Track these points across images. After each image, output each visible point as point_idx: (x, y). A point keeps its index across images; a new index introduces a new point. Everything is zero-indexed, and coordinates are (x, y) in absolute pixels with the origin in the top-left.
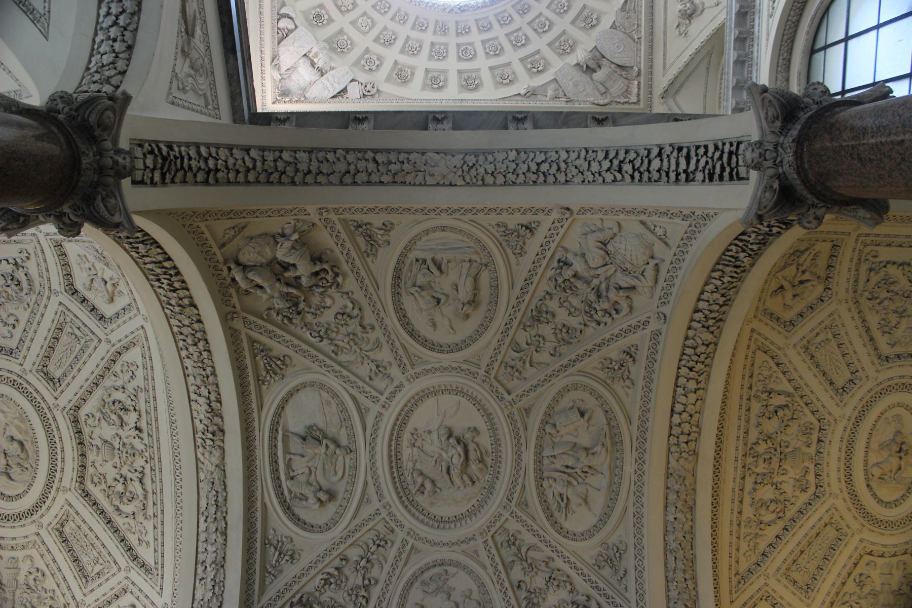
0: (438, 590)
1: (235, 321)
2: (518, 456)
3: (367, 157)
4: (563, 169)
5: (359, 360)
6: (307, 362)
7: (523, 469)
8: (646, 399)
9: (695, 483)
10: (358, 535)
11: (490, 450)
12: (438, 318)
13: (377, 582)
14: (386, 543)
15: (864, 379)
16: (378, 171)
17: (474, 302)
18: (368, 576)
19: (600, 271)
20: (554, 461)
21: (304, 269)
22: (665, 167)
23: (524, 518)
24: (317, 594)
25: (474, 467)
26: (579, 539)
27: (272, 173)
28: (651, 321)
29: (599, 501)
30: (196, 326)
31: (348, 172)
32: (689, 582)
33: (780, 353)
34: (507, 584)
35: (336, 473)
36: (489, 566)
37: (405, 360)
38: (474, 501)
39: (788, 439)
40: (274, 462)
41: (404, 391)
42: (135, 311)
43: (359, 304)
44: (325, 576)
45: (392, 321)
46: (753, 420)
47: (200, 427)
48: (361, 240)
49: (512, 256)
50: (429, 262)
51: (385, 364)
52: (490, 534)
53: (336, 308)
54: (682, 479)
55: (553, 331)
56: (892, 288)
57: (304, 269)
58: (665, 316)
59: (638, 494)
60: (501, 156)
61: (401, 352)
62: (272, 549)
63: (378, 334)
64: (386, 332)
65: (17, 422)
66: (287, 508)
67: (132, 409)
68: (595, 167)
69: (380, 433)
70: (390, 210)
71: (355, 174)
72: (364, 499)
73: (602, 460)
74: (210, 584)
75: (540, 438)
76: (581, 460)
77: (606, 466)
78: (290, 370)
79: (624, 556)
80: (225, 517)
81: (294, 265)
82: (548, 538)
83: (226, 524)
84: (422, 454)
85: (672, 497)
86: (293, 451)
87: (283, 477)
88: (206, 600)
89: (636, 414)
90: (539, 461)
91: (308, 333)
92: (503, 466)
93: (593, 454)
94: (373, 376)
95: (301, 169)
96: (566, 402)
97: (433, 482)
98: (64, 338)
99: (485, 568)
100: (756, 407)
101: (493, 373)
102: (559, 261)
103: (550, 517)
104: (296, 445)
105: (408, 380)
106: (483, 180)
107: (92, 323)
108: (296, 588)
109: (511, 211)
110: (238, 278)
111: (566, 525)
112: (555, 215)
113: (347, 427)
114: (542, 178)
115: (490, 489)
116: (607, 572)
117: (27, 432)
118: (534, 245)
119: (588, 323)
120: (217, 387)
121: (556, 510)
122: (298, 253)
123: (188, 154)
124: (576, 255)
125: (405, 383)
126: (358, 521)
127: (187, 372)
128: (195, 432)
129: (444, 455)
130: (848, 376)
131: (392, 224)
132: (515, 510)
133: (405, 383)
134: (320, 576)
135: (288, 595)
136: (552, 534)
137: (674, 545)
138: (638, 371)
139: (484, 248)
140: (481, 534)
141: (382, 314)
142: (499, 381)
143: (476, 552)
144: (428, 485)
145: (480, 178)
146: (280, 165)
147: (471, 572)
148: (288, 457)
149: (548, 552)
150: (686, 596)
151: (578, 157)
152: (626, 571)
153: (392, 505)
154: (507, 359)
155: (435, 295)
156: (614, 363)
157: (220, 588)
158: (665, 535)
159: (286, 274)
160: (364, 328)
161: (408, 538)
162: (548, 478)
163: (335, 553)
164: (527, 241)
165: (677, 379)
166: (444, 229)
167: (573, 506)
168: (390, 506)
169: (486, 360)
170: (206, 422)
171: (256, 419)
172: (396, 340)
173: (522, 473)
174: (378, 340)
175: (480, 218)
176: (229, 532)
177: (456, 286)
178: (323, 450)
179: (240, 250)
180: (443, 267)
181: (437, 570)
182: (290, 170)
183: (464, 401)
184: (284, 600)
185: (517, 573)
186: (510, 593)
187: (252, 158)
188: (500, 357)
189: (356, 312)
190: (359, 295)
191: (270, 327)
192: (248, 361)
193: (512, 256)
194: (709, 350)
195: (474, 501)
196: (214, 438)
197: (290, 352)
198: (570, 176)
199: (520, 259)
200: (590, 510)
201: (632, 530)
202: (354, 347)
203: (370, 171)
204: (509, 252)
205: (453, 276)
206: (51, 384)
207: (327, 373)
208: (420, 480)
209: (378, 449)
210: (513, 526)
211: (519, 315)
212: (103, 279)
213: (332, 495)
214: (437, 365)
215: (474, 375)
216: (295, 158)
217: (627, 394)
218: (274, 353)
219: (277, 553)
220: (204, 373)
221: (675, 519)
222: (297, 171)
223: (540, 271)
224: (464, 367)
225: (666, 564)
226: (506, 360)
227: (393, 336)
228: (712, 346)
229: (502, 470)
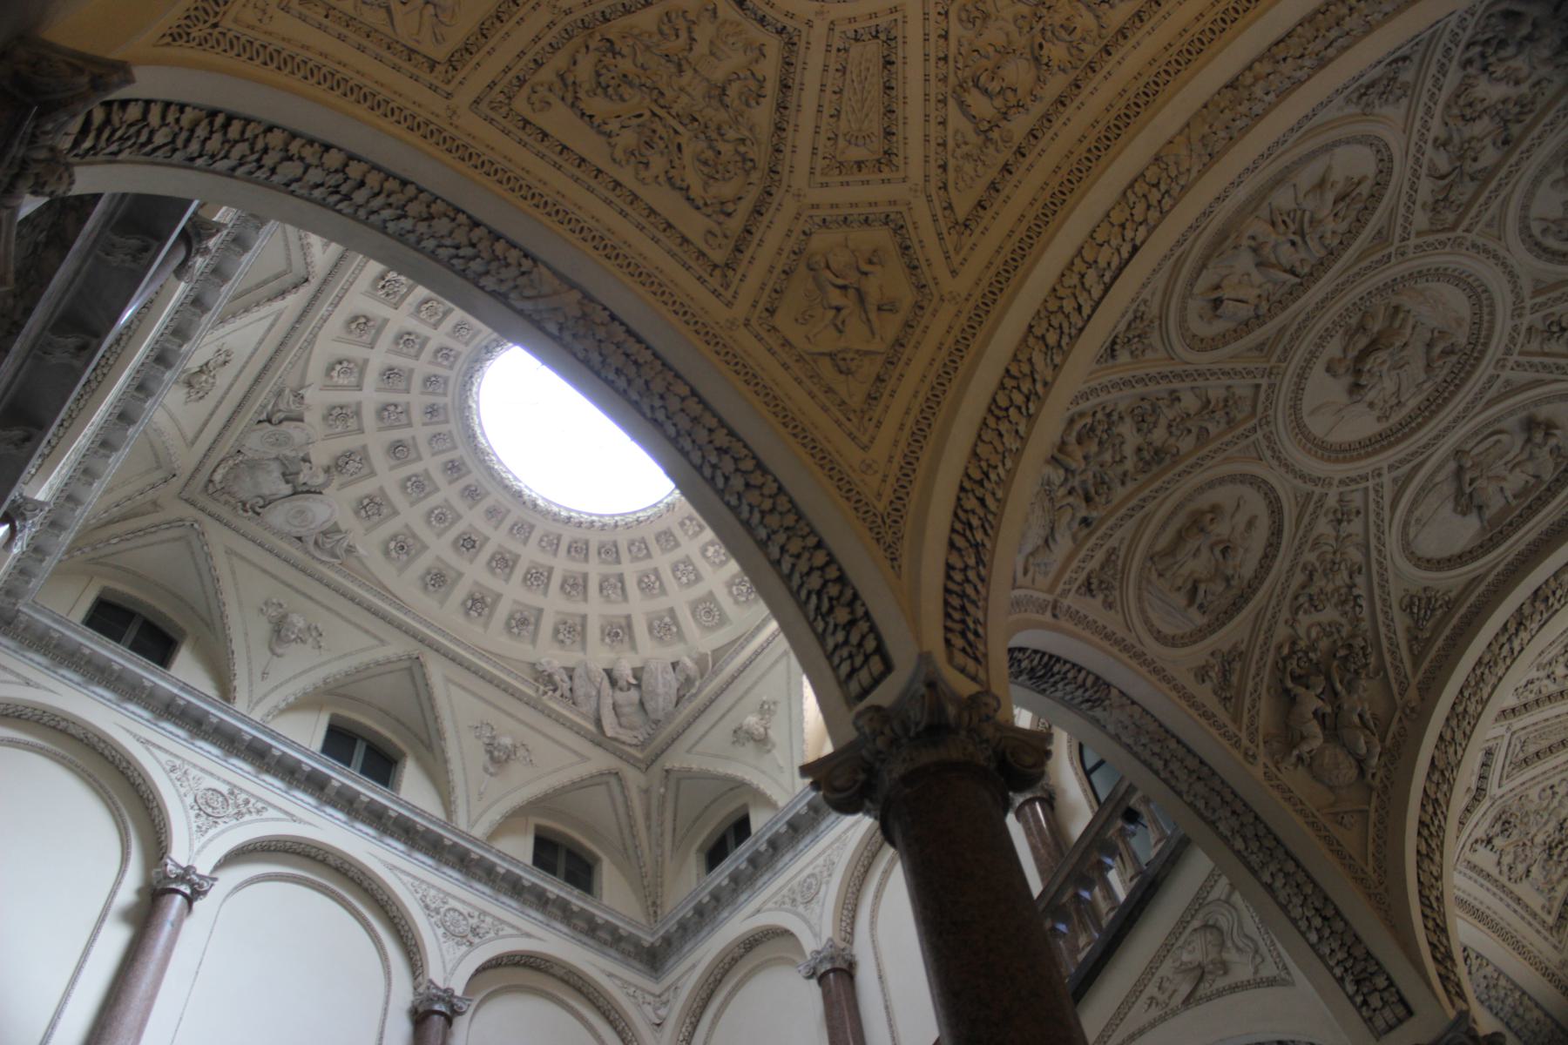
11: (1341, 331)
15: (838, 29)
23: (1400, 221)
30: (1448, 737)
33: (933, 190)
36: (1500, 198)
39: (1012, 28)
41: (1343, 476)
45: (1281, 563)
46: (1037, 109)
48: (1235, 679)
49: (1122, 553)
51: (1331, 516)
52: (1452, 235)
56: (710, 154)
57: (1311, 702)
63: (1310, 557)
64: (1299, 551)
72: (1512, 390)
90: (1313, 277)
97: (1430, 346)
98: (1532, 749)
100: (1019, 125)
115: (1391, 286)
121: (1358, 201)
125: (1336, 482)
130: (855, 50)
136: (1401, 171)
141: (1283, 579)
148: (1514, 503)
159: (1328, 709)
167: (1339, 187)
169: (1243, 443)
171: (1495, 572)
174: (1312, 549)
180: (1189, 585)
183: (1307, 405)
190: (1285, 614)
191: (1388, 657)
192: (1440, 643)
193: (1122, 553)
197: (1396, 612)
204: (1120, 563)
210: (1421, 219)
213: (1530, 424)
224: (1268, 453)
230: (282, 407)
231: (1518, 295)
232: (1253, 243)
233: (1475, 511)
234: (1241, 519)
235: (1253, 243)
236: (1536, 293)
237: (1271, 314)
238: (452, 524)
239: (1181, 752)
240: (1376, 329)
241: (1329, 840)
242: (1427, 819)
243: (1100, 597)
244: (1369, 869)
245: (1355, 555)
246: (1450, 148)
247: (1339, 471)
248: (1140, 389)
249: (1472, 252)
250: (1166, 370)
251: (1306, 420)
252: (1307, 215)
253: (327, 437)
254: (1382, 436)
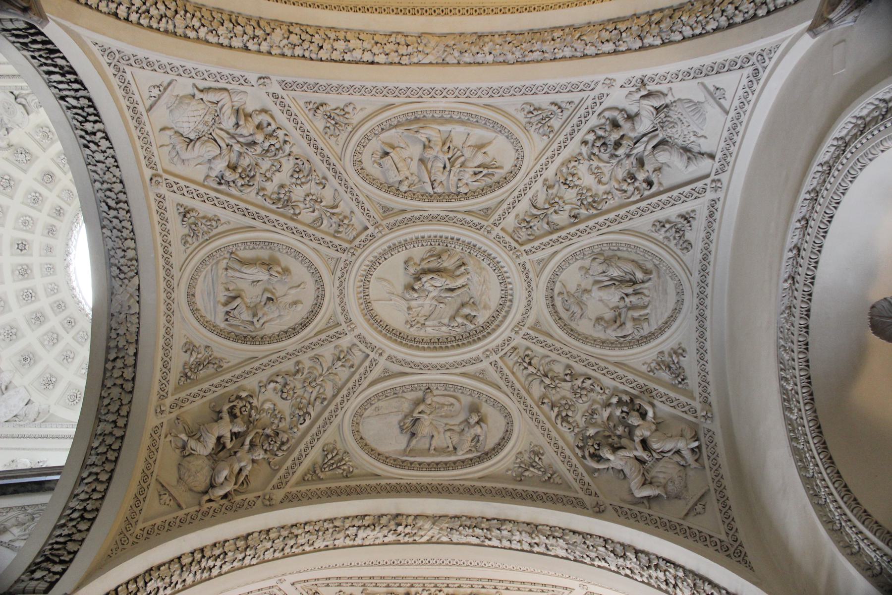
0: (580, 303)
1: (274, 497)
2: (432, 219)
3: (110, 368)
4: (109, 186)
5: (331, 377)
6: (331, 429)
7: (447, 213)
8: (362, 90)
9: (454, 34)
10: (517, 385)
11: (429, 247)
12: (289, 299)
13: (568, 367)
14: (527, 356)
16: (123, 357)
17: (268, 264)
18: (562, 376)
19: (223, 145)
20: (438, 181)
21: (225, 428)
22: (72, 93)
23: (500, 211)
24: (576, 430)
25: (448, 263)
26: (521, 154)
27: (107, 458)
28: (271, 91)
29: (479, 134)
30: (272, 535)
31: (122, 385)
32: (556, 35)
34: (573, 230)
35: (452, 404)
37: (332, 332)
38: (484, 264)
40: (437, 466)
41: (364, 333)
43: (272, 376)
44: (559, 421)
45: (290, 344)
47: (391, 537)
49: (220, 229)
50: (228, 308)
53: (277, 399)
54: (448, 49)
55: (299, 187)
57: (225, 428)
58: (260, 78)
59: (468, 94)
60: (110, 244)
61: (323, 336)
62: (526, 474)
63: (305, 359)
64: (304, 350)
66: (486, 456)
68: (99, 156)
69: (409, 358)
70: (167, 346)
71: (124, 379)
72: (480, 377)
73: (433, 132)
74: (551, 541)
75: (414, 197)
76: (435, 154)
77: (442, 128)
78: (339, 446)
79: (537, 106)
80: (488, 520)
81: (219, 438)
82: (522, 187)
83: (494, 519)
84: (433, 317)
85: (467, 58)
86: (427, 446)
87: (453, 458)
88: (566, 547)
89: (381, 101)
90: (439, 197)
91: (300, 426)
92: (444, 234)
93: (429, 141)
94: (348, 364)
95: (110, 430)
96: (374, 171)
97: (463, 305)
99: (556, 253)
101: (345, 245)
102: (220, 184)
103: (499, 184)
104: (420, 443)
105: (353, 329)
106: (131, 260)
108: (568, 452)
109: (165, 233)
110: (222, 492)
111: (508, 167)
112: (163, 190)
113: (403, 392)
114: (121, 205)
116: (556, 123)
118: (206, 209)
119: (287, 152)
120: (348, 518)
121: (491, 178)
122: (204, 435)
123: (57, 537)
124: (210, 168)
125: (356, 332)
126: (502, 384)
127: (331, 547)
128: (398, 543)
129: (432, 295)
131: (186, 344)
132: (491, 221)
133: (356, 332)
134: (559, 426)
135: (575, 461)
136: (518, 181)
137: (518, 54)
138: (334, 101)
139: (211, 256)
140: (518, 257)
141: (282, 354)
142: (355, 238)
143: (539, 262)
144: (466, 311)
145: (129, 263)
146: (102, 449)
147: (561, 268)
148: (432, 452)
149: (538, 186)
150: (569, 38)
151: (95, 172)
152: (552, 103)
153: (486, 348)
154: (332, 231)
155: (263, 303)
156: (328, 125)
157: (556, 531)
158: (508, 63)
160: (298, 371)
161: (522, 333)
162: (458, 188)
163: (536, 409)
164: (200, 215)
165: (335, 61)
166: (191, 296)
167: (487, 160)
168: (487, 350)
169: (332, 252)
170: (385, 532)
172: (310, 341)
173: (451, 215)
174: (311, 359)
175: (176, 261)
176: (502, 517)
177: (253, 282)
178: (425, 416)
179: (191, 490)
181: (558, 302)
182: (109, 440)
184: (578, 465)
185: (561, 218)
186: (582, 227)
187: (88, 476)
188: (328, 239)
189: (279, 379)
190: (263, 376)
194: (297, 30)
195: (484, 264)
196: (404, 524)
197: (319, 446)
198: (114, 179)
199: (223, 221)
200: (490, 143)
201: (507, 99)
202: (318, 381)
203: (122, 365)
204: (215, 231)
205: (244, 285)
207: (344, 410)
208: (459, 320)
209: (426, 361)
210: (510, 221)
211: (282, 220)
213: (474, 409)
214: (338, 300)
215: (347, 264)
216: (100, 435)
217: (361, 109)
218: (320, 461)
219: (532, 469)
220: (331, 531)
221: (490, 53)
222: (111, 433)
223: (233, 201)
224: (339, 274)
225: (538, 62)
226: (332, 232)
227: (307, 344)
228: (291, 29)
229: (449, 235)
230: (29, 99)
231: (524, 320)
232: (427, 143)
233: (409, 434)
234: (293, 294)
235: (427, 143)
236: (531, 328)
237: (405, 194)
238: (26, 231)
239: (130, 361)
240: (445, 264)
241: (142, 491)
242: (208, 553)
243: (186, 231)
244: (141, 525)
245: (329, 392)
246: (550, 191)
247: (363, 327)
248: (311, 151)
249: (521, 268)
250: (333, 160)
251: (373, 279)
252: (462, 159)
253: (29, 134)
254: (400, 334)
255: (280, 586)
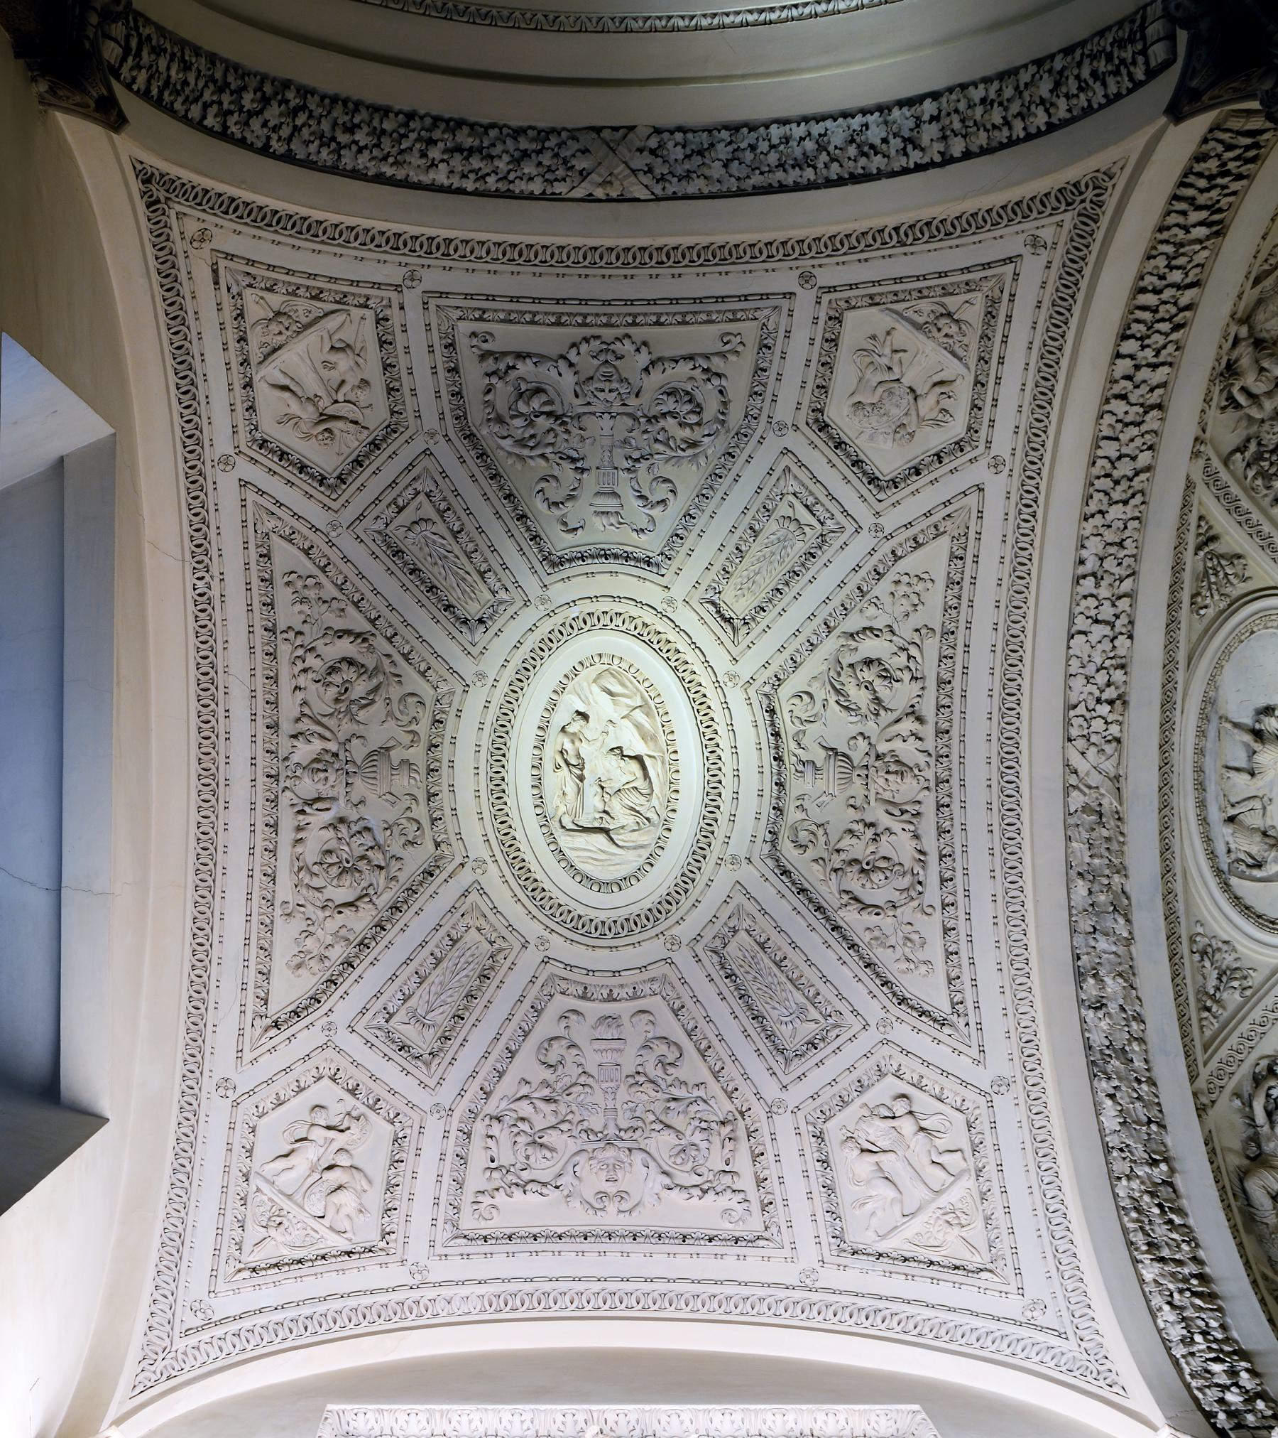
42: (981, 449)
65: (639, 716)
67: (906, 676)
87: (1215, 816)
107: (850, 494)
117: (654, 738)
206: (729, 630)
212: (912, 390)
219: (1215, 974)
255: (983, 462)
